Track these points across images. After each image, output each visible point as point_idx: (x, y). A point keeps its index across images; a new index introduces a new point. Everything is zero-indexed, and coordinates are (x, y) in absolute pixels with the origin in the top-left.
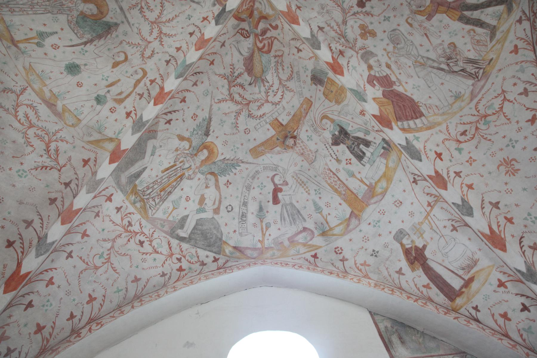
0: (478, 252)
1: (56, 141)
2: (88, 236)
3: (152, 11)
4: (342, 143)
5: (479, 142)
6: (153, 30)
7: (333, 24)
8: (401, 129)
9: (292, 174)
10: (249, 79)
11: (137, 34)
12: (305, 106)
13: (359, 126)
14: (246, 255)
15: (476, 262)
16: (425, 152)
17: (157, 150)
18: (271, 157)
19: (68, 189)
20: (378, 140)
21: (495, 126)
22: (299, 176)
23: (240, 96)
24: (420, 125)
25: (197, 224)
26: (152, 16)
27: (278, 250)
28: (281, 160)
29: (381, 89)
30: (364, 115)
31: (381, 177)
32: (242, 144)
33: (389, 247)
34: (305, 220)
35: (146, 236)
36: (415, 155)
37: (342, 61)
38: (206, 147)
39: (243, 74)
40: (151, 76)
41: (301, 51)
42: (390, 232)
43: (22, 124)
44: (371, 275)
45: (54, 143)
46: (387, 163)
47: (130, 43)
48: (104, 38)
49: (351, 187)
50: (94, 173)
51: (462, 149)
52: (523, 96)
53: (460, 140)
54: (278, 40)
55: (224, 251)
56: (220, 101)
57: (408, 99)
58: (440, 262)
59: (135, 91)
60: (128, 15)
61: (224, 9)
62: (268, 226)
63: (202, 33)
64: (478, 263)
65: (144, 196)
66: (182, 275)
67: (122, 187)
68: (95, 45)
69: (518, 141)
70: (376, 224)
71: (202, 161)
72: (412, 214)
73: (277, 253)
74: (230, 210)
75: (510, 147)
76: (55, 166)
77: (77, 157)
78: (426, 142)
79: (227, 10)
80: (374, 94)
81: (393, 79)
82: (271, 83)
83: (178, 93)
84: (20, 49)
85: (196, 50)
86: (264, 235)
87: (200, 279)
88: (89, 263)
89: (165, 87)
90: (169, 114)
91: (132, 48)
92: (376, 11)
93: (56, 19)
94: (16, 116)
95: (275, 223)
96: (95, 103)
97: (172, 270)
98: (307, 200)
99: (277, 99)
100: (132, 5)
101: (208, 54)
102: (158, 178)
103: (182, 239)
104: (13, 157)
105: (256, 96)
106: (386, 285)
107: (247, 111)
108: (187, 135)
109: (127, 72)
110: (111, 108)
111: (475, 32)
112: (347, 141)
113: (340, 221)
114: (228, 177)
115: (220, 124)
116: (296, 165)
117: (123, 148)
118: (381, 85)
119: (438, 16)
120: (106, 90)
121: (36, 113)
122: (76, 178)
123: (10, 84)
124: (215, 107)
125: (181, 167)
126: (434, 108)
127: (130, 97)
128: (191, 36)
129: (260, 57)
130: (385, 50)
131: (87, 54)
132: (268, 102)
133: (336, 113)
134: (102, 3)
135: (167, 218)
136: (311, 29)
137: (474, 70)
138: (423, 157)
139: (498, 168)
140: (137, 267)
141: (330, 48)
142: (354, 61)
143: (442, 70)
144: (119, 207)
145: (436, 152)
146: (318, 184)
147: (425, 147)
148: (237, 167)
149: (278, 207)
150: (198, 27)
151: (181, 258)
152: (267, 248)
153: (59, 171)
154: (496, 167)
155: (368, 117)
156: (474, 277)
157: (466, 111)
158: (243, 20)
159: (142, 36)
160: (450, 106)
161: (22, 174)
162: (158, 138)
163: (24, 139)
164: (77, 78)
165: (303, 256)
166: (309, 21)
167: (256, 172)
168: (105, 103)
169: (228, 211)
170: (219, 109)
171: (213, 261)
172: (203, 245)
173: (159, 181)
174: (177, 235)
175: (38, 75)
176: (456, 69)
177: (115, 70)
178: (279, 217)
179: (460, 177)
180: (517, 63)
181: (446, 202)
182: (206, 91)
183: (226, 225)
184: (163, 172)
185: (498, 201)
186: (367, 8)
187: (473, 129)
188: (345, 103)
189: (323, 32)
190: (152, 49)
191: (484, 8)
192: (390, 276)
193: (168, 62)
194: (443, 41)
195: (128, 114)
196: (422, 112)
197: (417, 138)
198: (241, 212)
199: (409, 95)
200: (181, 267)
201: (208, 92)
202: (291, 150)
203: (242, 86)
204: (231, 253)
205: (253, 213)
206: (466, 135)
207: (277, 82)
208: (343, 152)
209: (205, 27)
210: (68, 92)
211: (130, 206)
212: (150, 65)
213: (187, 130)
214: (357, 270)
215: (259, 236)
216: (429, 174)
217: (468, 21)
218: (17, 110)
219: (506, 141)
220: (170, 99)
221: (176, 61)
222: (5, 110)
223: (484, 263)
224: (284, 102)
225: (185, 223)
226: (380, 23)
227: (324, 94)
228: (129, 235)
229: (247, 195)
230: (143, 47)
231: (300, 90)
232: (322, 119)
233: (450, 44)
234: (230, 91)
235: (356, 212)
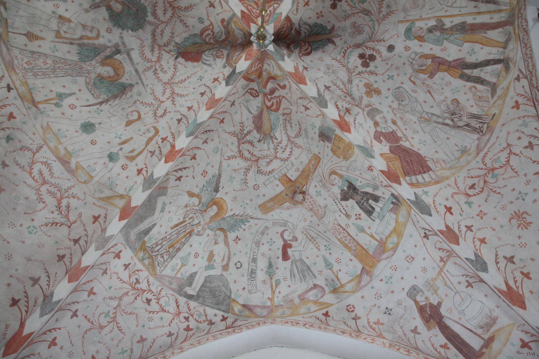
0: (496, 309)
1: (67, 197)
2: (94, 294)
3: (165, 72)
4: (351, 198)
5: (488, 196)
7: (339, 83)
8: (409, 184)
9: (301, 230)
10: (258, 136)
12: (313, 162)
13: (368, 182)
14: (255, 314)
15: (494, 320)
16: (435, 206)
17: (167, 207)
18: (281, 213)
19: (77, 245)
20: (387, 196)
21: (504, 179)
22: (308, 231)
23: (250, 152)
24: (428, 180)
25: (205, 281)
26: (165, 77)
27: (289, 308)
28: (290, 215)
29: (388, 144)
30: (372, 170)
31: (391, 232)
32: (251, 200)
33: (403, 304)
34: (315, 277)
35: (153, 294)
36: (425, 210)
37: (349, 119)
38: (215, 203)
39: (252, 131)
40: (162, 134)
41: (308, 109)
42: (403, 289)
43: (36, 181)
44: (385, 334)
45: (67, 199)
46: (397, 217)
49: (361, 243)
50: (104, 230)
51: (472, 203)
52: (529, 149)
53: (469, 193)
54: (286, 98)
55: (233, 309)
56: (229, 158)
57: (415, 154)
58: (456, 320)
59: (147, 149)
60: (143, 77)
61: (234, 71)
62: (278, 283)
63: (213, 93)
64: (497, 321)
65: (152, 252)
66: (189, 335)
67: (131, 244)
68: (110, 105)
69: (527, 194)
70: (389, 280)
71: (212, 217)
72: (424, 270)
73: (288, 312)
74: (239, 266)
75: (520, 200)
76: (66, 223)
77: (88, 213)
78: (435, 196)
79: (237, 71)
80: (381, 149)
81: (400, 134)
82: (279, 140)
83: (189, 151)
84: (40, 110)
85: (207, 109)
86: (274, 292)
87: (208, 339)
88: (94, 322)
89: (176, 145)
90: (179, 171)
92: (380, 70)
94: (31, 173)
95: (285, 279)
96: (107, 160)
97: (179, 329)
98: (317, 256)
99: (285, 155)
101: (219, 113)
102: (167, 234)
103: (190, 297)
104: (25, 213)
105: (266, 153)
106: (401, 345)
107: (256, 167)
108: (196, 191)
109: (139, 130)
111: (476, 89)
112: (356, 196)
113: (351, 278)
114: (237, 233)
115: (229, 181)
116: (305, 220)
117: (133, 205)
118: (388, 141)
119: (439, 75)
120: (119, 147)
121: (50, 170)
122: (86, 235)
123: (27, 142)
124: (225, 164)
125: (190, 223)
126: (442, 162)
127: (142, 154)
128: (202, 96)
129: (269, 115)
130: (390, 106)
131: (102, 113)
132: (277, 158)
133: (344, 169)
135: (176, 275)
136: (318, 88)
137: (478, 125)
138: (433, 212)
139: (510, 222)
140: (143, 326)
141: (337, 106)
142: (360, 119)
143: (447, 125)
144: (127, 264)
145: (446, 207)
146: (328, 240)
147: (434, 201)
148: (246, 223)
149: (288, 263)
150: (209, 88)
151: (188, 317)
152: (277, 306)
153: (69, 227)
154: (507, 220)
155: (376, 173)
156: (494, 336)
157: (473, 164)
158: (253, 81)
159: (155, 96)
160: (457, 160)
161: (33, 230)
162: (168, 194)
163: (37, 195)
164: (91, 137)
165: (314, 314)
166: (316, 81)
167: (266, 227)
168: (117, 160)
169: (237, 268)
170: (229, 166)
171: (222, 320)
172: (212, 303)
173: (168, 237)
174: (185, 293)
175: (54, 133)
176: (460, 124)
177: (128, 128)
178: (289, 274)
179: (472, 231)
180: (519, 118)
181: (460, 257)
183: (235, 282)
184: (172, 228)
185: (512, 255)
186: (372, 67)
187: (482, 183)
188: (353, 158)
189: (330, 91)
190: (165, 109)
191: (483, 67)
192: (405, 335)
193: (179, 121)
194: (446, 98)
195: (139, 172)
196: (430, 167)
197: (426, 193)
198: (250, 269)
199: (416, 150)
200: (188, 326)
202: (300, 205)
203: (251, 143)
204: (240, 312)
205: (262, 270)
206: (475, 189)
207: (285, 139)
208: (353, 207)
209: (216, 87)
210: (82, 149)
211: (138, 263)
212: (162, 124)
213: (197, 186)
214: (371, 330)
215: (269, 294)
216: (439, 229)
217: (469, 79)
219: (516, 193)
220: (180, 156)
221: (187, 120)
222: (21, 168)
223: (503, 321)
224: (292, 159)
225: (193, 280)
226: (384, 81)
227: (332, 150)
228: (136, 293)
229: (256, 251)
230: (156, 106)
231: (308, 146)
232: (330, 175)
233: (453, 100)
234: (239, 149)
235: (367, 268)
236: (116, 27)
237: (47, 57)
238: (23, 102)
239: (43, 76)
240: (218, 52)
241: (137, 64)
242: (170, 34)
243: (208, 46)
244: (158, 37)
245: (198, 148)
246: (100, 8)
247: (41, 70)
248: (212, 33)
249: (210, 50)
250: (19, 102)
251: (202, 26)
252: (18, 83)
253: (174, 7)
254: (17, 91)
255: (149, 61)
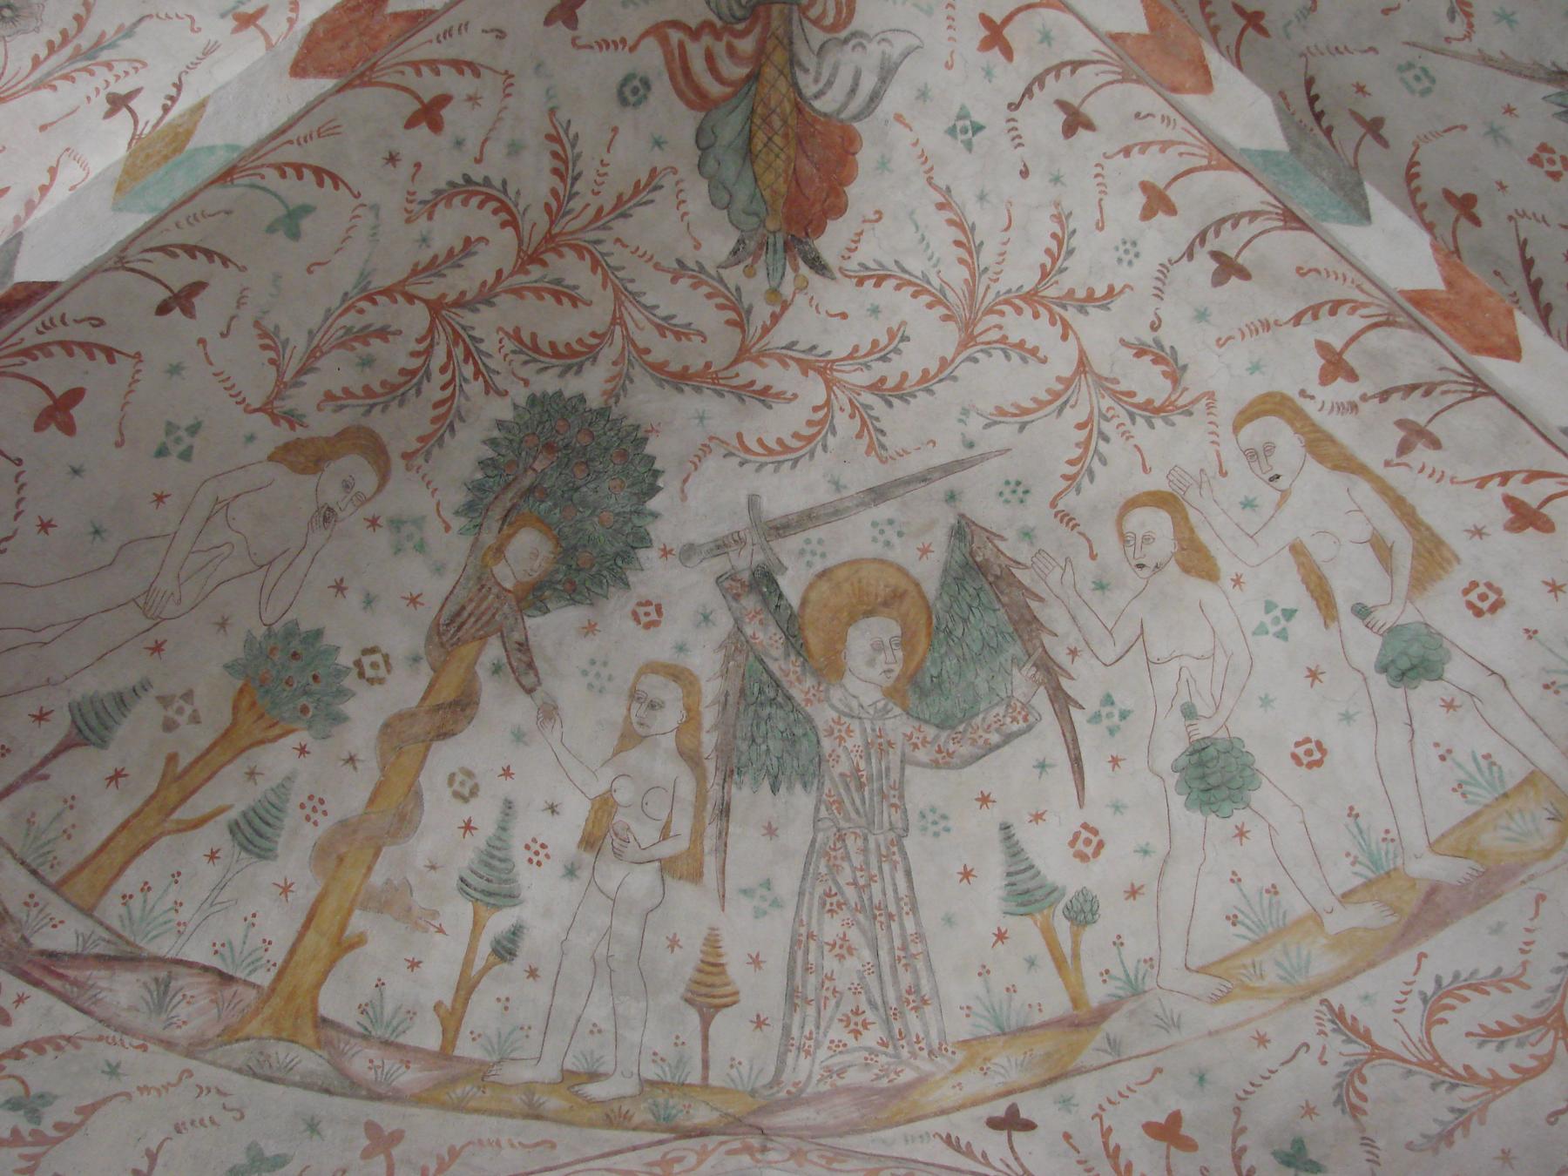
3: (898, 336)
6: (1014, 338)
11: (1022, 427)
43: (1546, 1063)
47: (1072, 470)
48: (1034, 604)
59: (1377, 467)
60: (914, 464)
68: (1073, 653)
84: (1119, 1002)
85: (1206, 84)
89: (1409, 286)
90: (1546, 295)
91: (1104, 462)
93: (931, 817)
94: (1497, 1083)
96: (1426, 693)
100: (859, 436)
109: (1248, 504)
110: (1470, 605)
121: (1478, 988)
124: (1495, 39)
127: (1411, 498)
128: (1089, 126)
131: (1123, 700)
134: (847, 587)
150: (1040, 80)
159: (1041, 404)
164: (1273, 764)
170: (1506, 18)
175: (1257, 943)
177: (1227, 567)
182: (1409, 75)
193: (1227, 268)
201: (1410, 66)
210: (1352, 814)
218: (1461, 1071)
221: (1235, 219)
222: (1465, 1125)
230: (1107, 402)
236: (632, 578)
237: (810, 936)
238: (1080, 1071)
239: (920, 964)
240: (814, 13)
241: (837, 485)
242: (684, 283)
243: (769, 72)
244: (693, 356)
245: (1411, 177)
246: (532, 639)
247: (886, 970)
248: (707, 40)
249: (793, 61)
250: (1086, 1090)
251: (662, 88)
252: (974, 1083)
253: (549, 237)
254: (1023, 1089)
255: (822, 422)
